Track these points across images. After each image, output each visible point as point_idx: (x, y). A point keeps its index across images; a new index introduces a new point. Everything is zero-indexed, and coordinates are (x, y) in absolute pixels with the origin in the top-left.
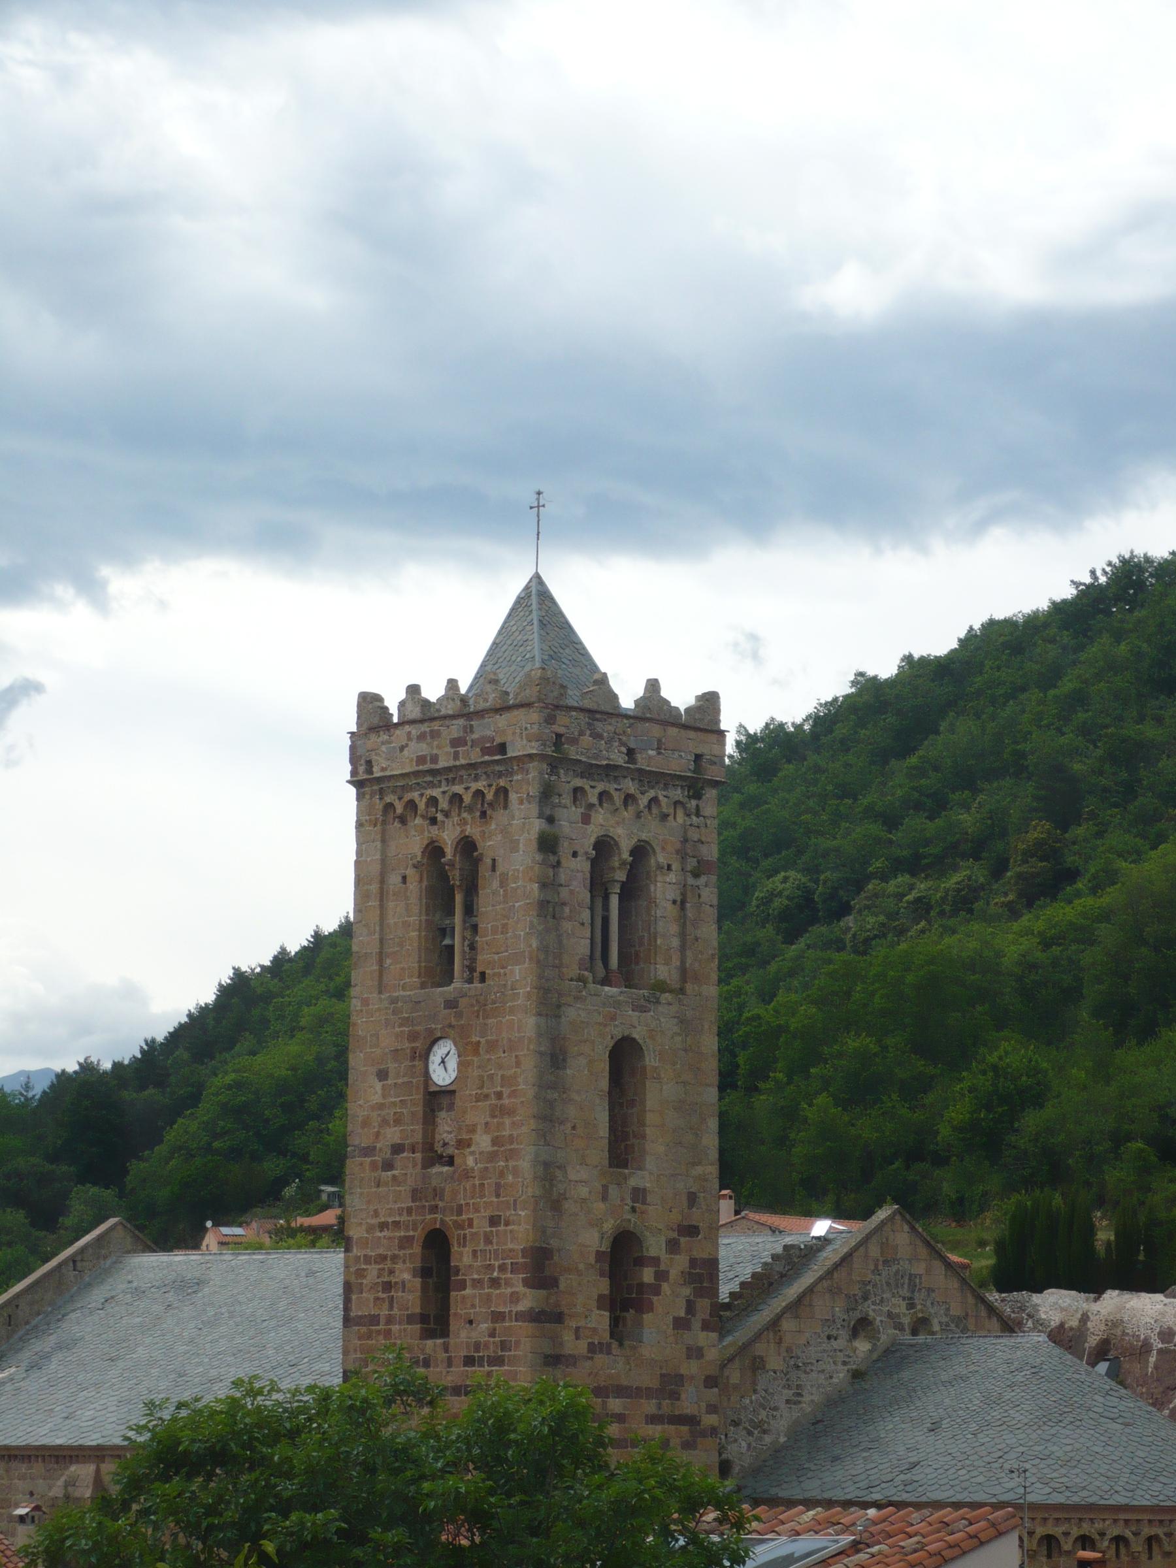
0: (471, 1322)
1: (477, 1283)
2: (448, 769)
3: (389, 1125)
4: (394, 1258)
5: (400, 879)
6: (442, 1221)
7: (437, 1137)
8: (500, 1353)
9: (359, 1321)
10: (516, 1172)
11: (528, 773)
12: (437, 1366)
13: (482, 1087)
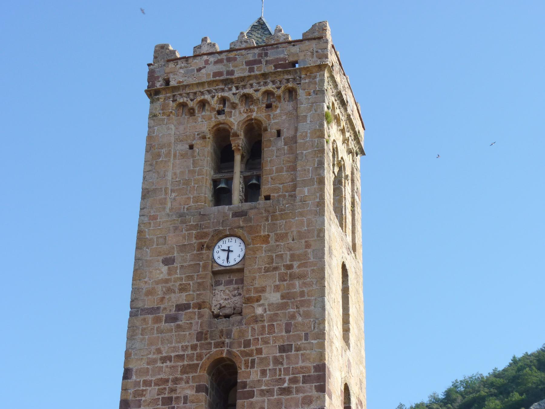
1: (263, 393)
2: (242, 79)
3: (174, 292)
4: (176, 381)
5: (188, 147)
6: (229, 352)
7: (214, 303)
11: (315, 77)
13: (272, 263)
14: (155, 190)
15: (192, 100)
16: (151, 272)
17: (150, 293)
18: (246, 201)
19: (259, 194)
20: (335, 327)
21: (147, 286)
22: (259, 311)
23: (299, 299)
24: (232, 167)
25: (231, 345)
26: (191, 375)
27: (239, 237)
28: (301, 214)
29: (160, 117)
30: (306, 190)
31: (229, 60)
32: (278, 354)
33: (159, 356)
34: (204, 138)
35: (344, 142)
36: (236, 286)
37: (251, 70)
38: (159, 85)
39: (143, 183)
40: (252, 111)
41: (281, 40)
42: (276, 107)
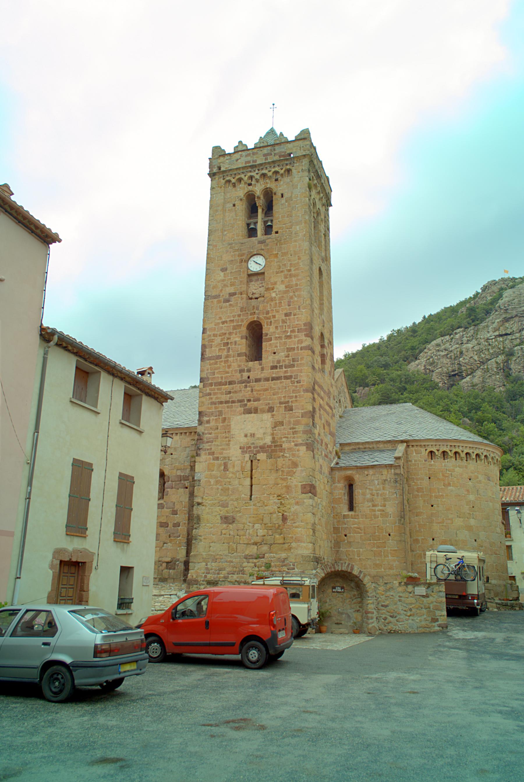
0: (275, 353)
1: (276, 338)
2: (261, 165)
3: (228, 286)
4: (230, 334)
6: (258, 318)
7: (249, 291)
8: (292, 363)
9: (210, 358)
10: (299, 296)
11: (302, 162)
12: (255, 371)
14: (215, 231)
15: (234, 178)
16: (214, 276)
17: (214, 287)
18: (265, 235)
19: (272, 231)
20: (315, 302)
21: (213, 283)
22: (274, 295)
23: (295, 288)
24: (257, 216)
25: (259, 314)
26: (238, 330)
27: (262, 255)
28: (295, 241)
29: (217, 189)
30: (298, 227)
31: (253, 154)
32: (284, 318)
33: (220, 321)
34: (241, 200)
35: (320, 200)
36: (261, 282)
37: (266, 159)
38: (215, 170)
39: (209, 227)
40: (267, 183)
41: (283, 141)
42: (280, 180)
